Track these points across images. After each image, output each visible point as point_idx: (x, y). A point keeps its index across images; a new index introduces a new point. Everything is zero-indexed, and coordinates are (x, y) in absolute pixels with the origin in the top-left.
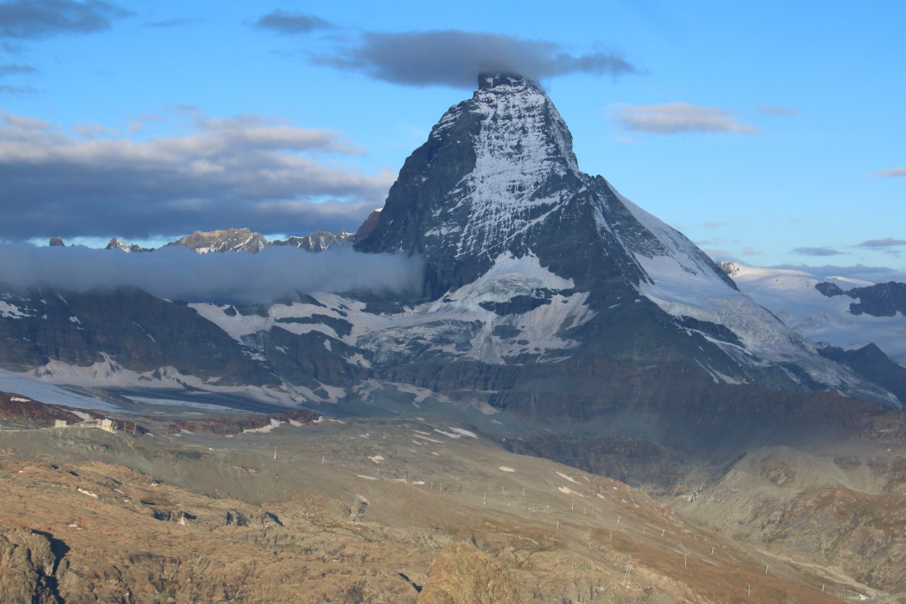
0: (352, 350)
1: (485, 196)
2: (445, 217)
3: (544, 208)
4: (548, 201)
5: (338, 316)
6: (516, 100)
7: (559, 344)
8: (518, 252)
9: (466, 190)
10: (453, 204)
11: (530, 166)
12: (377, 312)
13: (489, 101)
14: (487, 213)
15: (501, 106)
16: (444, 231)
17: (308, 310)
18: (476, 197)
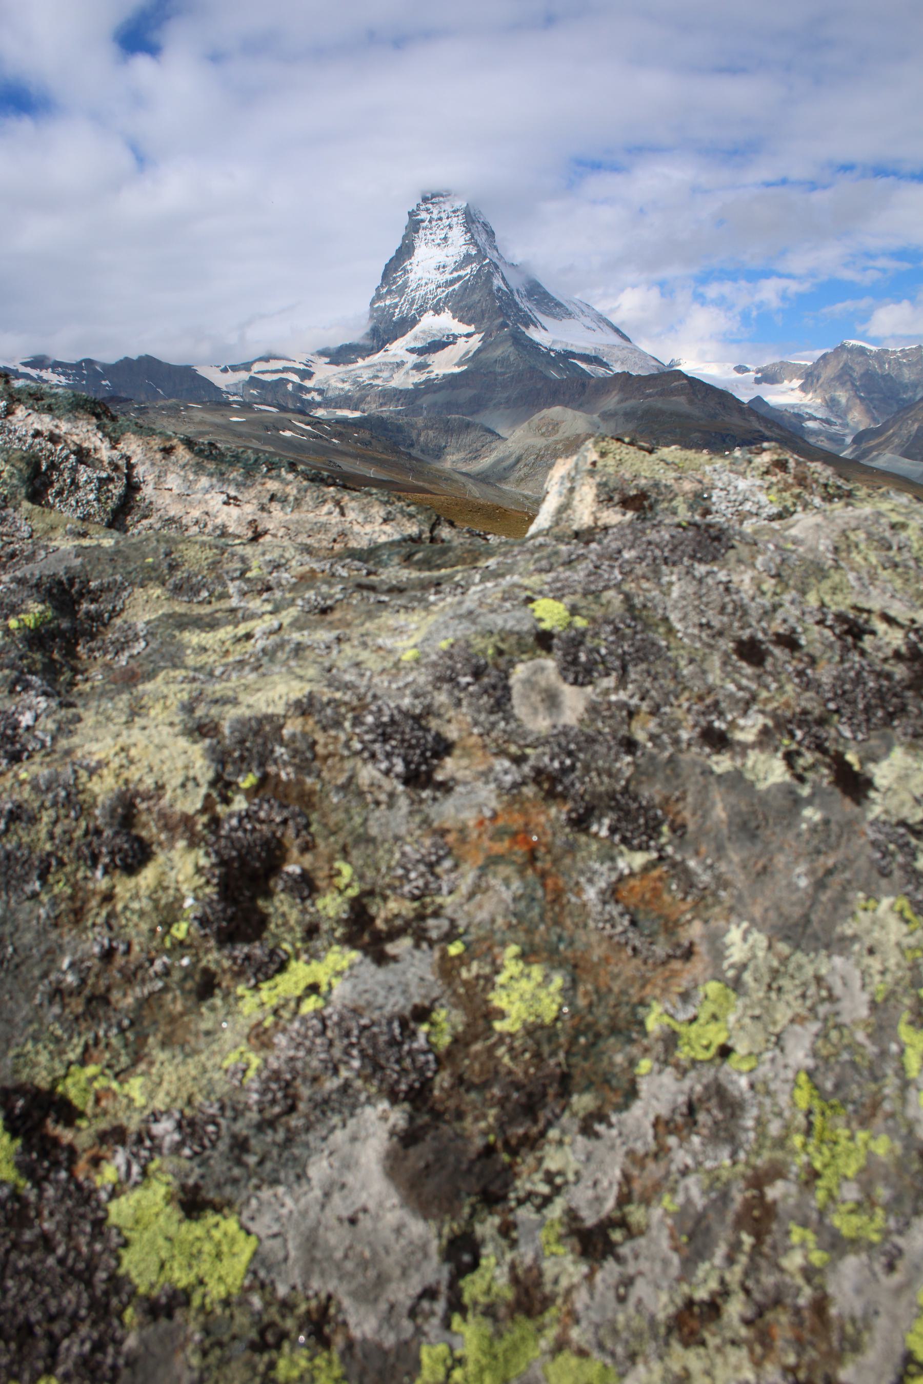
0: (309, 390)
1: (419, 275)
2: (389, 292)
3: (460, 278)
4: (462, 273)
5: (302, 367)
6: (447, 207)
7: (457, 370)
8: (437, 311)
9: (406, 272)
10: (395, 283)
11: (451, 250)
12: (337, 364)
13: (427, 210)
14: (419, 286)
15: (435, 212)
16: (388, 302)
17: (279, 365)
18: (412, 276)
